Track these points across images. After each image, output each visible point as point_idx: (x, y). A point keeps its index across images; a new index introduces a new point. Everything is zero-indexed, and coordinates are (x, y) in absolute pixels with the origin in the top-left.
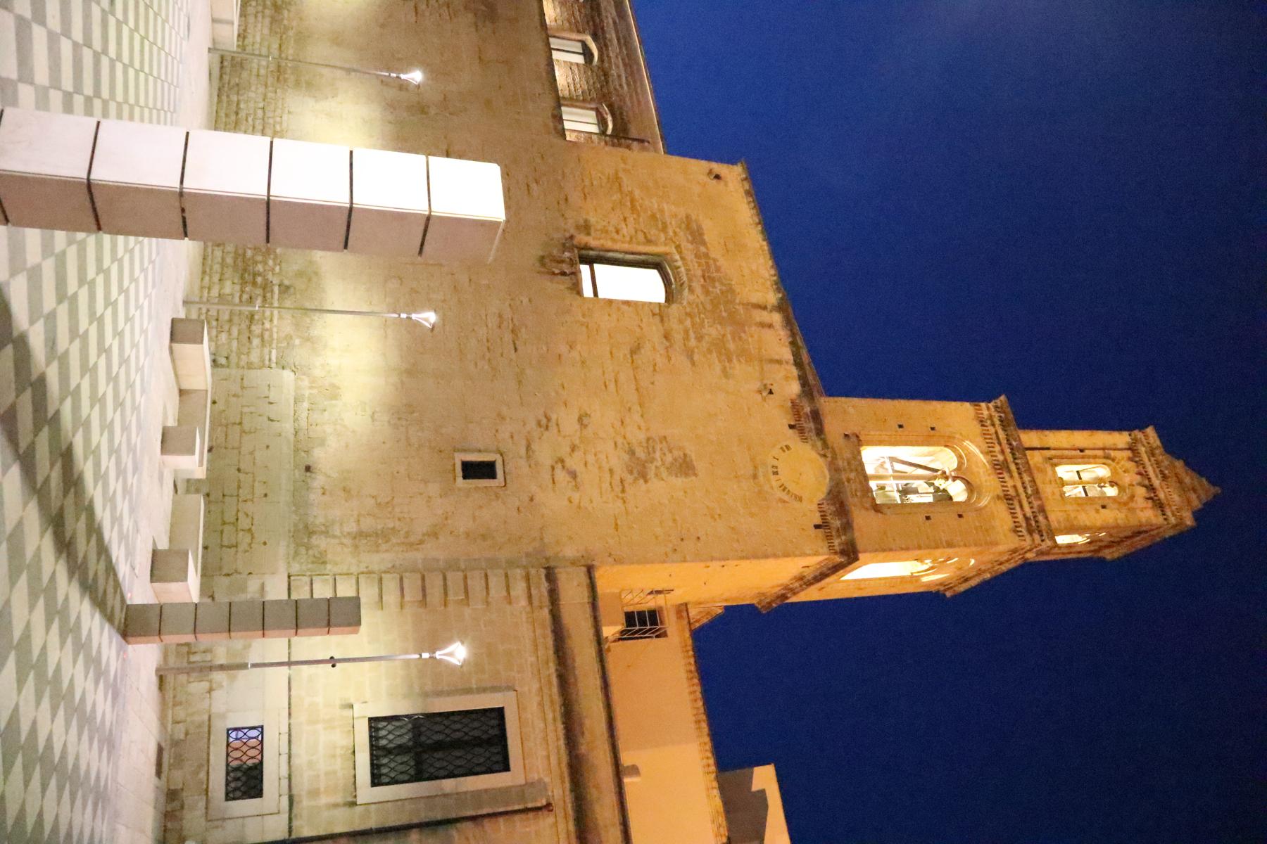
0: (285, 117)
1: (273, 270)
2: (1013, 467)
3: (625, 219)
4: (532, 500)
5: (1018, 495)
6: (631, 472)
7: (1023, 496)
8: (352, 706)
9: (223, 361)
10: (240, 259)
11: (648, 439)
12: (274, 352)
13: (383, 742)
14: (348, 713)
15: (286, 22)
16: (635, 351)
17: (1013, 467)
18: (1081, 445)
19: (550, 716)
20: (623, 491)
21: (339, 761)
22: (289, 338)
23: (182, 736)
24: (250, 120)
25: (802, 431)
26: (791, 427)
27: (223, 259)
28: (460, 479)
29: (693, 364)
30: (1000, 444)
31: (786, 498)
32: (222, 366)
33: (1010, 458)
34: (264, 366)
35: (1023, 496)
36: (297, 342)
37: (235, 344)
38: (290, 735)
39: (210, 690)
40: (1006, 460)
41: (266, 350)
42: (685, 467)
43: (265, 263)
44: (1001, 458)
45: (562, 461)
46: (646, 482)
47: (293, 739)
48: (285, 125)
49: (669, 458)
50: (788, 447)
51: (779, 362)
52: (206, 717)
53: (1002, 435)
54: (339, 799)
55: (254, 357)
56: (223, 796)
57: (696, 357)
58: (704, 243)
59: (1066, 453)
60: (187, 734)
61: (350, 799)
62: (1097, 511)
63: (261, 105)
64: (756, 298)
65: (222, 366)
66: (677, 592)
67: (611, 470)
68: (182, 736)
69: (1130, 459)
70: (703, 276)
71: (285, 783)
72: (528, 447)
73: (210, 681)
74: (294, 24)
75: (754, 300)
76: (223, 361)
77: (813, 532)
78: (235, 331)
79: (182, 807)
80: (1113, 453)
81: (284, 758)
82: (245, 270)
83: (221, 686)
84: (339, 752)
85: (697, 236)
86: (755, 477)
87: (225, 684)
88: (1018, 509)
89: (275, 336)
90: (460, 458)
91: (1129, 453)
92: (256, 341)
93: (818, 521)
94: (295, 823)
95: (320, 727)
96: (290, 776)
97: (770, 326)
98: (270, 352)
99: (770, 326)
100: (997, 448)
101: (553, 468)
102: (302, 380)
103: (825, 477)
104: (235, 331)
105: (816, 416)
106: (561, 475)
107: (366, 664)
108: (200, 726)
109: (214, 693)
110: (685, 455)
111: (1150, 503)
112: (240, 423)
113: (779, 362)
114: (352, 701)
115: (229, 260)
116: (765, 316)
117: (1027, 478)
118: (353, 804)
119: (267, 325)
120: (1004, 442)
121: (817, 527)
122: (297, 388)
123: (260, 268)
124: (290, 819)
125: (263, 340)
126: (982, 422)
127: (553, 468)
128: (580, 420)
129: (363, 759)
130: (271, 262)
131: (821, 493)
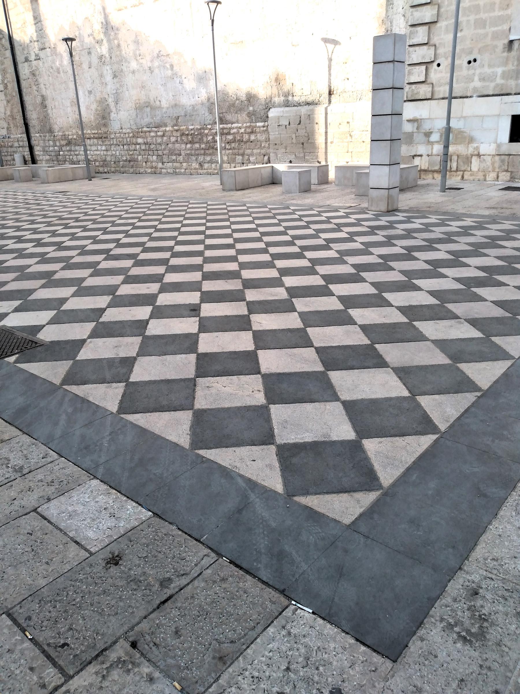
0: (124, 131)
1: (210, 129)
8: (511, 42)
10: (207, 152)
15: (75, 137)
22: (249, 115)
23: (509, 174)
24: (131, 153)
27: (208, 162)
32: (269, 158)
34: (267, 130)
36: (251, 108)
37: (255, 151)
39: (479, 155)
41: (258, 130)
43: (207, 135)
48: (128, 131)
52: (497, 158)
60: (507, 171)
63: (122, 147)
65: (269, 158)
68: (509, 174)
73: (472, 155)
74: (74, 131)
76: (266, 158)
78: (248, 151)
83: (477, 148)
87: (475, 145)
89: (248, 124)
92: (253, 137)
98: (259, 127)
102: (274, 103)
104: (248, 151)
108: (503, 161)
109: (482, 152)
112: (303, 144)
114: (506, 41)
115: (208, 158)
119: (242, 130)
122: (279, 106)
125: (252, 132)
130: (206, 131)
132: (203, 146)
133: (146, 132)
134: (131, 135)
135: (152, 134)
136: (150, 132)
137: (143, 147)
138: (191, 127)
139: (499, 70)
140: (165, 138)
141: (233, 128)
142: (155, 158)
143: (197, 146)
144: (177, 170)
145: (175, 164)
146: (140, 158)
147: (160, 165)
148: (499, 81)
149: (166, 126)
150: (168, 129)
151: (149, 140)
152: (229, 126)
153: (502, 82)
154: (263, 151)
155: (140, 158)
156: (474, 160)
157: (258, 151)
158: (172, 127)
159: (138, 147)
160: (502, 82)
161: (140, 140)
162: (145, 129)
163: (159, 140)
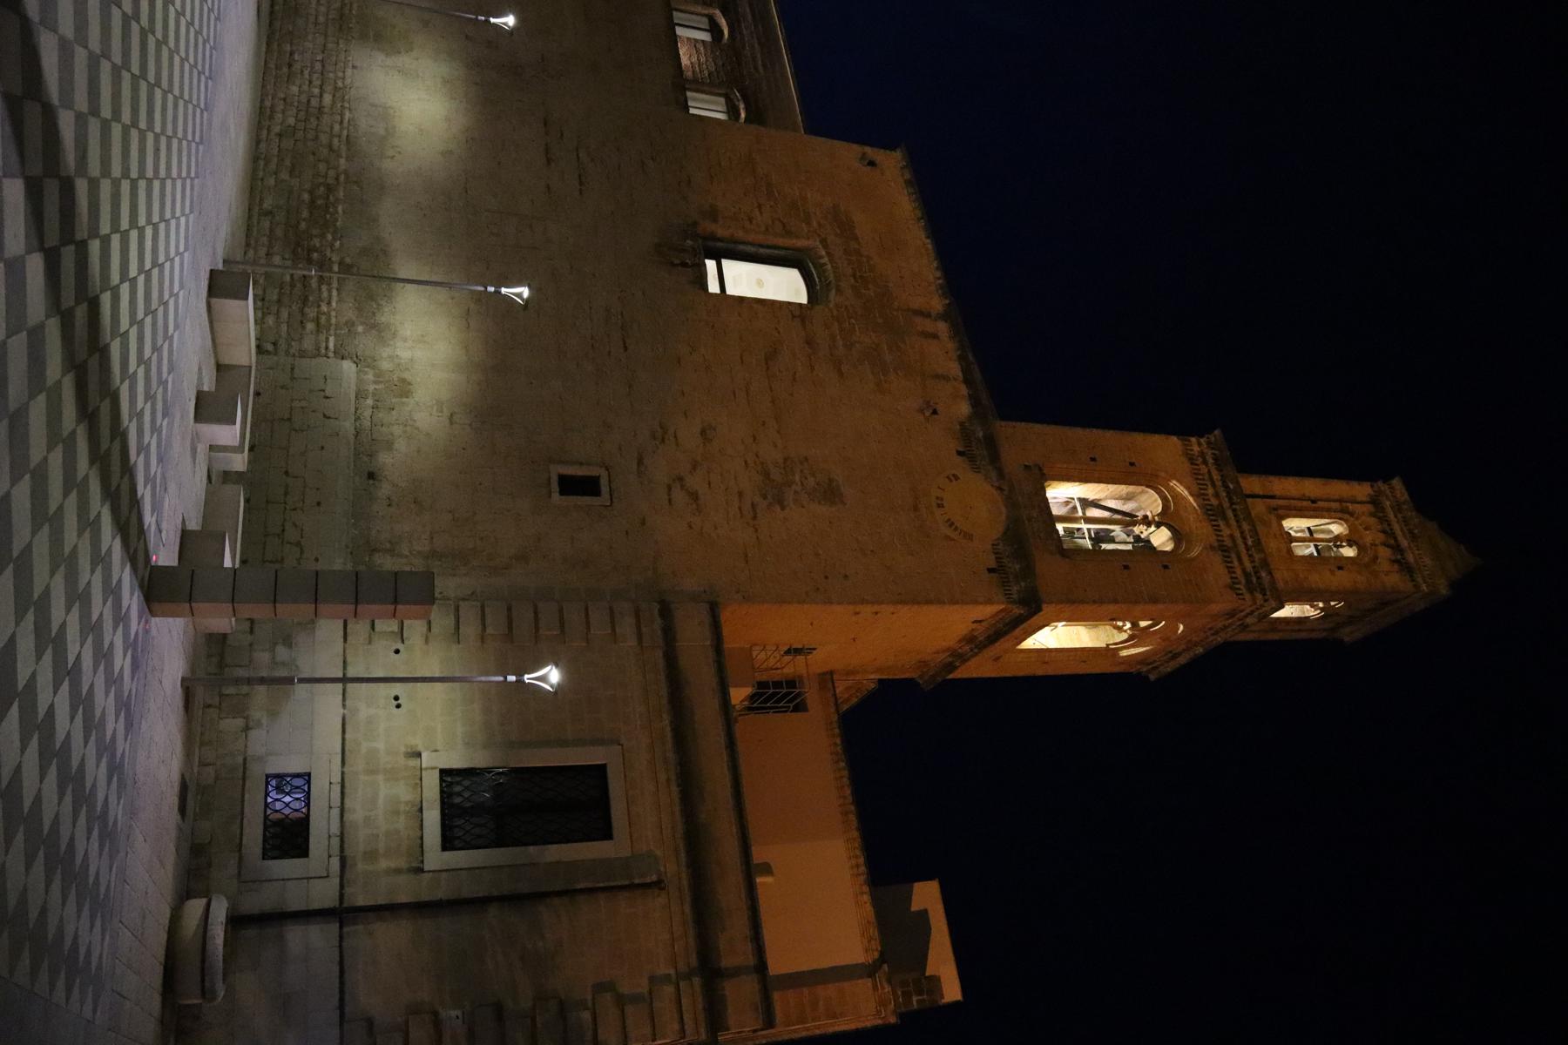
0: (349, 72)
1: (332, 246)
2: (1230, 514)
3: (760, 206)
4: (643, 523)
5: (1236, 545)
6: (765, 497)
7: (1242, 548)
8: (419, 755)
9: (270, 347)
11: (786, 460)
12: (332, 339)
13: (457, 800)
14: (414, 762)
16: (771, 357)
17: (1230, 514)
18: (1313, 496)
19: (663, 777)
20: (755, 518)
21: (402, 818)
24: (306, 72)
26: (960, 453)
27: (271, 230)
28: (556, 496)
29: (841, 374)
30: (1214, 485)
31: (953, 535)
33: (1226, 505)
35: (1242, 548)
36: (360, 329)
37: (284, 328)
38: (343, 787)
39: (247, 728)
40: (1221, 505)
41: (322, 337)
42: (830, 493)
43: (323, 236)
44: (1214, 502)
45: (681, 479)
46: (783, 508)
47: (347, 791)
48: (348, 81)
49: (811, 481)
50: (957, 478)
51: (946, 378)
52: (240, 759)
53: (1216, 476)
54: (402, 863)
55: (308, 344)
56: (258, 850)
57: (844, 368)
58: (856, 239)
60: (217, 778)
61: (415, 865)
62: (1332, 572)
63: (319, 57)
64: (917, 303)
65: (268, 352)
66: (816, 656)
67: (740, 494)
69: (1373, 515)
70: (854, 276)
71: (336, 842)
72: (640, 462)
73: (247, 718)
75: (916, 307)
76: (270, 347)
78: (285, 314)
79: (210, 865)
80: (1351, 507)
81: (336, 812)
82: (298, 244)
83: (259, 724)
84: (402, 807)
85: (846, 228)
86: (916, 509)
87: (264, 721)
88: (1236, 563)
89: (333, 321)
90: (557, 469)
91: (1370, 507)
92: (310, 326)
93: (993, 564)
94: (347, 890)
95: (380, 777)
96: (342, 834)
97: (935, 336)
98: (327, 340)
99: (935, 336)
100: (1210, 491)
101: (669, 488)
104: (285, 314)
105: (991, 443)
106: (679, 496)
107: (438, 685)
109: (253, 734)
110: (831, 480)
111: (1396, 567)
113: (946, 378)
114: (420, 748)
115: (279, 232)
116: (928, 325)
117: (1246, 527)
118: (420, 870)
119: (324, 308)
120: (1219, 483)
121: (990, 570)
122: (360, 381)
123: (316, 242)
124: (342, 886)
125: (318, 325)
126: (1192, 460)
127: (669, 488)
128: (703, 432)
129: (433, 817)
130: (329, 237)
132: (303, 225)
133: (342, 115)
134: (340, 84)
135: (337, 127)
136: (341, 122)
137: (314, 102)
138: (340, 209)
139: (380, 745)
140: (326, 151)
141: (330, 291)
142: (291, 121)
143: (305, 214)
144: (262, 163)
145: (275, 160)
146: (295, 89)
147: (277, 129)
148: (365, 747)
149: (347, 159)
150: (342, 161)
151: (326, 119)
152: (335, 285)
153: (364, 751)
154: (282, 342)
155: (295, 89)
156: (240, 722)
157: (284, 334)
158: (346, 172)
159: (316, 91)
160: (364, 751)
161: (327, 99)
162: (347, 115)
163: (324, 138)
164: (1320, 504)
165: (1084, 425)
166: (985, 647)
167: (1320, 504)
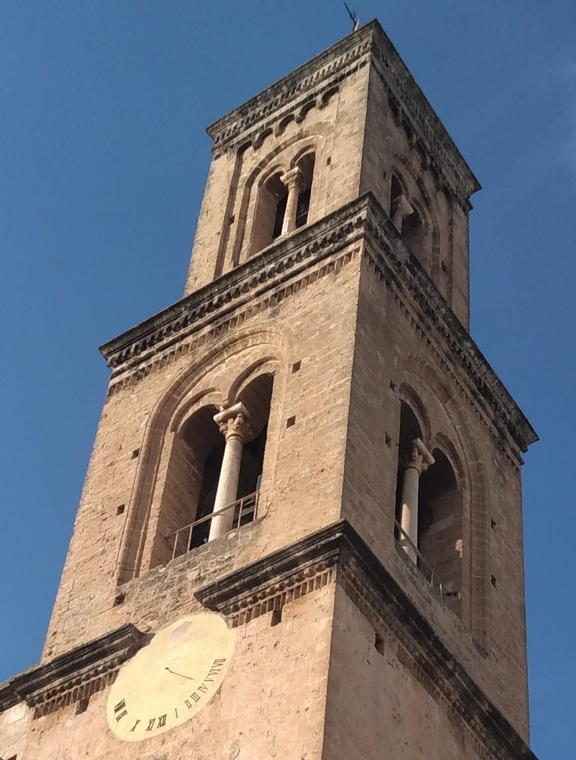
5: (274, 285)
25: (97, 687)
31: (212, 690)
50: (121, 705)
59: (231, 243)
77: (286, 625)
80: (245, 174)
93: (268, 616)
100: (189, 340)
103: (187, 625)
105: (69, 663)
131: (215, 621)
164: (236, 211)
165: (70, 532)
166: (439, 645)
167: (236, 211)
